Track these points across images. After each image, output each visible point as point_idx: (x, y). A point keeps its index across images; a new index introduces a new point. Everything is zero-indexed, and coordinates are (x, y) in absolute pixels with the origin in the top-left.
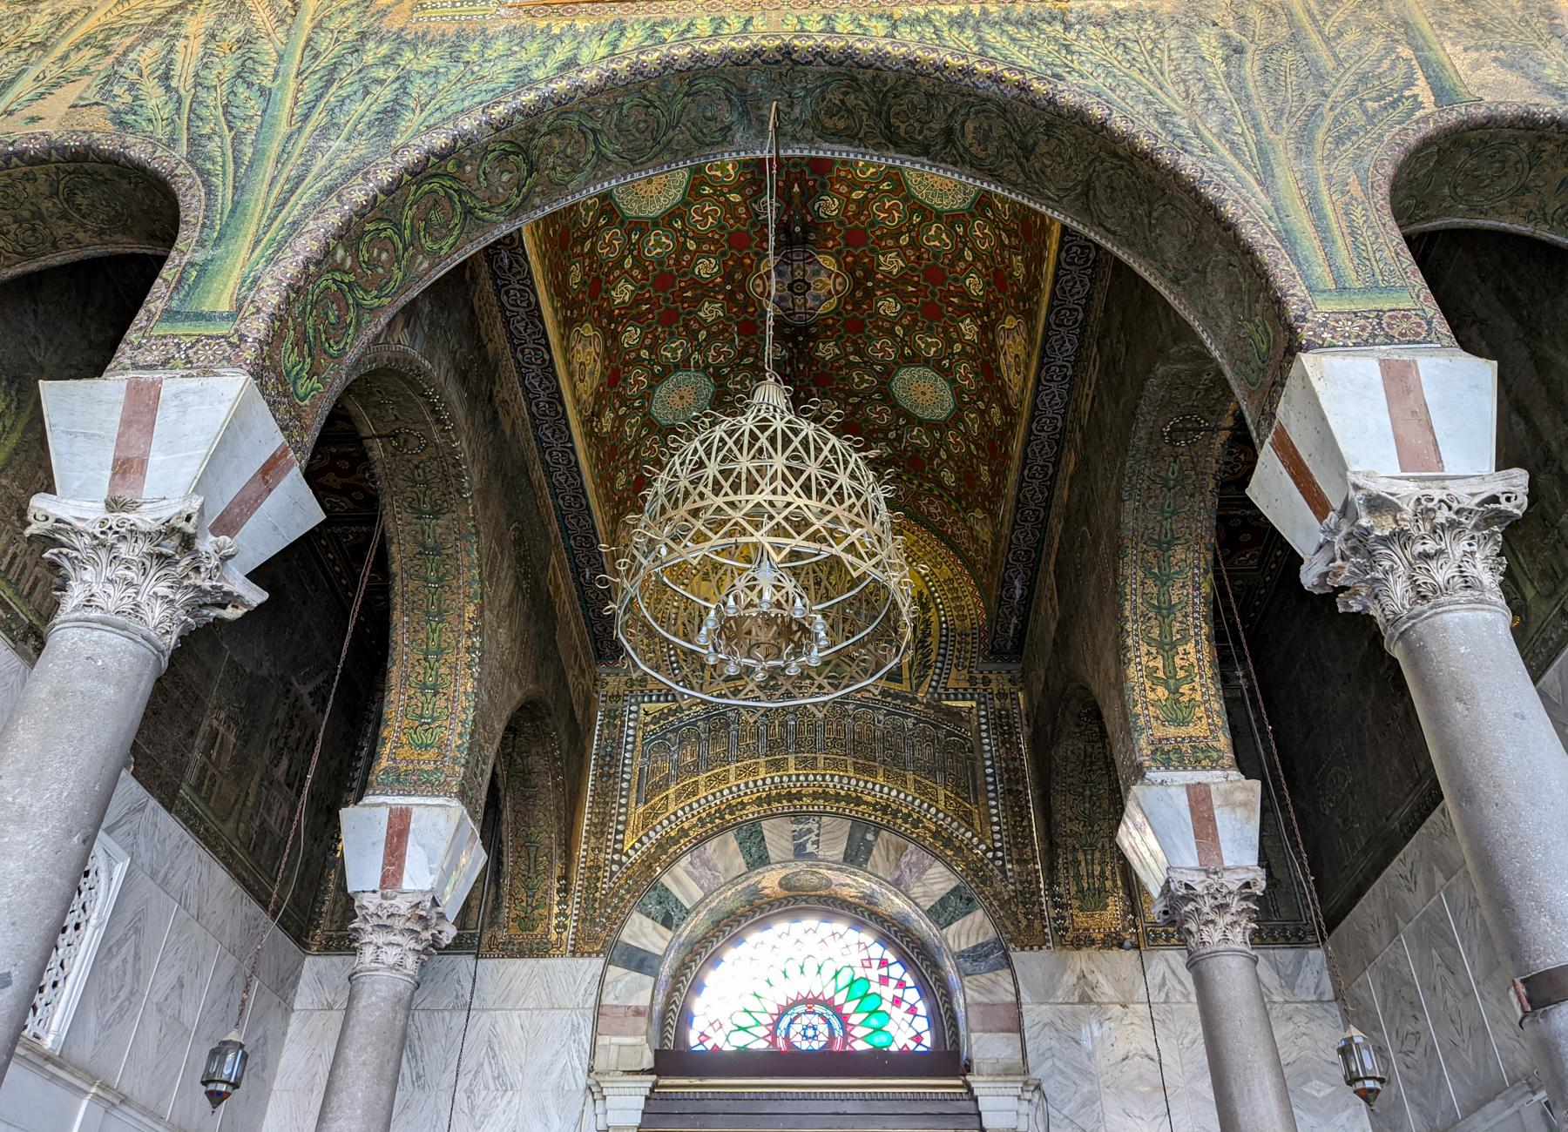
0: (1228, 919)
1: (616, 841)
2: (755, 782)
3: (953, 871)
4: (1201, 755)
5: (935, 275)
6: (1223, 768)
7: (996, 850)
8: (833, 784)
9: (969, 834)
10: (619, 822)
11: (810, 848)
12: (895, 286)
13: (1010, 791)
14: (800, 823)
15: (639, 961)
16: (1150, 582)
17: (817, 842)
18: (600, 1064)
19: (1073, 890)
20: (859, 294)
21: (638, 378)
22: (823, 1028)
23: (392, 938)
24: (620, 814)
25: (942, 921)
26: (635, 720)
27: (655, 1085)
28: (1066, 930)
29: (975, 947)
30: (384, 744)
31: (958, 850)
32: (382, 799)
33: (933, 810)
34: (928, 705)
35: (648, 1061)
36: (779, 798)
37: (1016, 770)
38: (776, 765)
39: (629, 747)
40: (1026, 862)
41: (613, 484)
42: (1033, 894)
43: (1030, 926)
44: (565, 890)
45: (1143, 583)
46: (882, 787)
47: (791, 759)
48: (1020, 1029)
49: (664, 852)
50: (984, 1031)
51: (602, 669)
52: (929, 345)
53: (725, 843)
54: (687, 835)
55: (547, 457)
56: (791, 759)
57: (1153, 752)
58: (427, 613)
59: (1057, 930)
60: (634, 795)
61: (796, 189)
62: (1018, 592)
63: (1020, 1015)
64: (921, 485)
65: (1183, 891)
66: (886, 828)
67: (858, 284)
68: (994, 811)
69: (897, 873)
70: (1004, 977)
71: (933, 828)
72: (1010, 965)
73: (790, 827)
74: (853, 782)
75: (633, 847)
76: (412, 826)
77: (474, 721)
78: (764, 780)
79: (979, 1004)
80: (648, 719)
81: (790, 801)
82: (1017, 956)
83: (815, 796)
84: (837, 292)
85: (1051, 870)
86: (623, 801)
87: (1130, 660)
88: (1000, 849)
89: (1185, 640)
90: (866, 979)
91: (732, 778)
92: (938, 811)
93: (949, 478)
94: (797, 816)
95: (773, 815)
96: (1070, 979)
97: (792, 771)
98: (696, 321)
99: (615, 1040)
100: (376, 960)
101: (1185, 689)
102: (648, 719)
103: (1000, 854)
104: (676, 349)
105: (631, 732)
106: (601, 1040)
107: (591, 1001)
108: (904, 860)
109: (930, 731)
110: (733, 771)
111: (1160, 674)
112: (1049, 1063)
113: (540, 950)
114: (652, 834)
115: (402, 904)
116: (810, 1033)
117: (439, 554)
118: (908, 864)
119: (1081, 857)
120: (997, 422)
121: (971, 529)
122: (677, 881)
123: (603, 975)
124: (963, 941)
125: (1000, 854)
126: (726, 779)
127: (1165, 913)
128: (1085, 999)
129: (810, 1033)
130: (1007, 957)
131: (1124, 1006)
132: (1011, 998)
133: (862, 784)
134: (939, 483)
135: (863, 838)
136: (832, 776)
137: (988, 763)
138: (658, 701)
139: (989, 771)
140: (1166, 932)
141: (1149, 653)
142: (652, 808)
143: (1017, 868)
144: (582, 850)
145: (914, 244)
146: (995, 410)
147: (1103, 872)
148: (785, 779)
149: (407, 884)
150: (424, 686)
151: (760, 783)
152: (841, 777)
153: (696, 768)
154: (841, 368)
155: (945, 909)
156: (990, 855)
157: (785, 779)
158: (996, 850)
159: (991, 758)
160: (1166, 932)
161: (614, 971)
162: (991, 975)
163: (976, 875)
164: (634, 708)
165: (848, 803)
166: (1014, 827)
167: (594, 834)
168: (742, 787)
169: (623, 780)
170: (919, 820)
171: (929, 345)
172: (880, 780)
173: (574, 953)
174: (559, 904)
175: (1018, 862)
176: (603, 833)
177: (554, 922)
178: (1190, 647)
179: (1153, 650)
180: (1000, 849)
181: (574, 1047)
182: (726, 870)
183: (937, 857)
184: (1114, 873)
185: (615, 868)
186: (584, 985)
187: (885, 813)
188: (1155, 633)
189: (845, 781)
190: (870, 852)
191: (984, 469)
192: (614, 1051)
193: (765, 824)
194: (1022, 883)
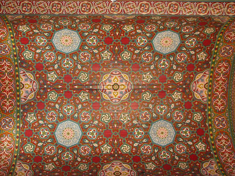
5: (108, 41)
12: (116, 54)
64: (219, 41)
93: (209, 31)
134: (214, 34)
145: (97, 47)
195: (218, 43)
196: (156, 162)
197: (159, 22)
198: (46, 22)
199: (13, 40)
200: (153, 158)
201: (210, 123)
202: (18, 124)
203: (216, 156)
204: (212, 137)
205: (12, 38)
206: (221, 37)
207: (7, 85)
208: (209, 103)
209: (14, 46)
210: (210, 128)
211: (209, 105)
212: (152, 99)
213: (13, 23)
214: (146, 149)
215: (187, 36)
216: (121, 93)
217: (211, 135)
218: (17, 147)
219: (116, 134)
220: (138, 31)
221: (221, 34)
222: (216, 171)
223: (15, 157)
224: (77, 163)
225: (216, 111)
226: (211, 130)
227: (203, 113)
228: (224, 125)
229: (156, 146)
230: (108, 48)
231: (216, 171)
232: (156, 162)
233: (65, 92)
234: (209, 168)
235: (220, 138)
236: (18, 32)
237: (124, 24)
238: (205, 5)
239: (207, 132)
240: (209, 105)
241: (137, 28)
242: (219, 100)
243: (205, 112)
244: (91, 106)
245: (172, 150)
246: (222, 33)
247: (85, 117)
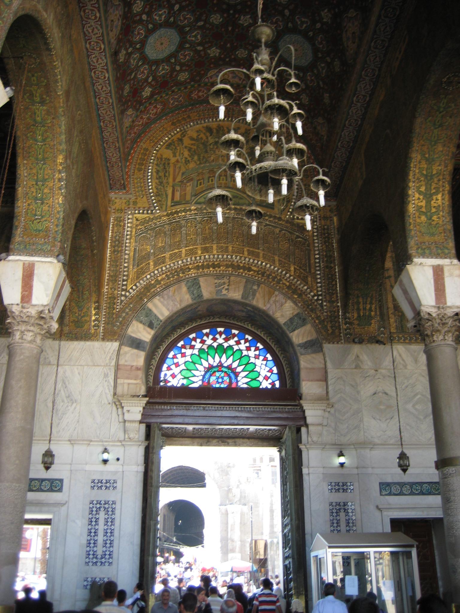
0: (446, 329)
1: (123, 285)
2: (196, 257)
3: (296, 305)
4: (440, 251)
6: (450, 258)
7: (318, 296)
8: (236, 259)
9: (306, 287)
10: (124, 276)
11: (224, 292)
13: (327, 267)
14: (219, 279)
15: (137, 344)
16: (423, 162)
18: (119, 390)
19: (356, 315)
21: (140, 31)
22: (226, 379)
23: (29, 328)
24: (124, 271)
26: (131, 223)
27: (148, 403)
28: (351, 334)
29: (306, 342)
30: (17, 229)
31: (300, 295)
32: (18, 258)
33: (288, 275)
34: (287, 222)
35: (143, 391)
36: (208, 267)
37: (331, 257)
38: (205, 250)
39: (128, 237)
40: (333, 302)
41: (123, 92)
42: (336, 317)
43: (333, 332)
44: (98, 308)
45: (420, 162)
46: (262, 263)
47: (215, 246)
48: (326, 380)
49: (148, 292)
50: (308, 380)
51: (112, 195)
52: (302, 23)
53: (180, 288)
54: (160, 283)
55: (93, 74)
56: (215, 246)
57: (417, 249)
58: (37, 159)
59: (346, 334)
60: (132, 262)
65: (427, 316)
66: (263, 283)
68: (319, 277)
69: (268, 306)
70: (318, 357)
71: (288, 284)
73: (213, 281)
74: (247, 259)
75: (132, 288)
76: (36, 272)
77: (63, 218)
78: (200, 257)
79: (307, 368)
80: (138, 223)
81: (214, 268)
82: (327, 347)
83: (227, 266)
85: (345, 306)
86: (126, 265)
87: (409, 202)
88: (321, 295)
89: (437, 193)
90: (248, 356)
91: (183, 255)
92: (290, 276)
94: (218, 276)
95: (206, 275)
96: (351, 357)
97: (215, 252)
99: (127, 381)
100: (22, 338)
101: (435, 218)
102: (138, 223)
103: (320, 298)
104: (161, 15)
105: (129, 229)
106: (119, 381)
107: (113, 363)
108: (273, 299)
109: (288, 235)
110: (183, 250)
111: (424, 210)
112: (339, 395)
113: (86, 337)
114: (141, 282)
115: (33, 312)
116: (220, 380)
117: (44, 126)
119: (361, 300)
120: (337, 69)
121: (315, 128)
122: (156, 306)
123: (119, 350)
124: (300, 339)
125: (320, 298)
126: (180, 256)
127: (415, 326)
128: (357, 367)
129: (220, 380)
131: (376, 371)
133: (251, 261)
135: (251, 288)
136: (236, 256)
137: (317, 252)
138: (143, 213)
139: (317, 256)
140: (398, 337)
141: (419, 199)
142: (142, 268)
144: (105, 289)
146: (337, 63)
147: (371, 308)
148: (212, 257)
149: (34, 301)
150: (36, 199)
151: (198, 258)
152: (241, 257)
153: (163, 250)
155: (292, 323)
156: (316, 298)
157: (212, 257)
158: (318, 296)
159: (318, 250)
160: (398, 337)
161: (125, 349)
163: (308, 307)
164: (130, 217)
165: (244, 270)
166: (328, 284)
167: (112, 281)
168: (189, 259)
169: (126, 254)
170: (280, 280)
171: (302, 23)
172: (261, 259)
173: (103, 339)
174: (95, 315)
175: (329, 302)
176: (116, 281)
177: (93, 324)
178: (439, 197)
179: (421, 197)
180: (321, 295)
181: (106, 384)
182: (181, 301)
183: (289, 298)
184: (376, 308)
185: (123, 298)
186: (110, 355)
187: (263, 276)
188: (423, 189)
189: (243, 259)
191: (326, 95)
192: (126, 387)
193: (202, 280)
194: (330, 312)
208: (202, 85)
210: (170, 93)
211: (199, 85)
217: (161, 97)
225: (191, 92)
226: (167, 94)
227: (188, 81)
235: (158, 107)
239: (164, 92)
240: (199, 85)
242: (206, 93)
243: (189, 83)
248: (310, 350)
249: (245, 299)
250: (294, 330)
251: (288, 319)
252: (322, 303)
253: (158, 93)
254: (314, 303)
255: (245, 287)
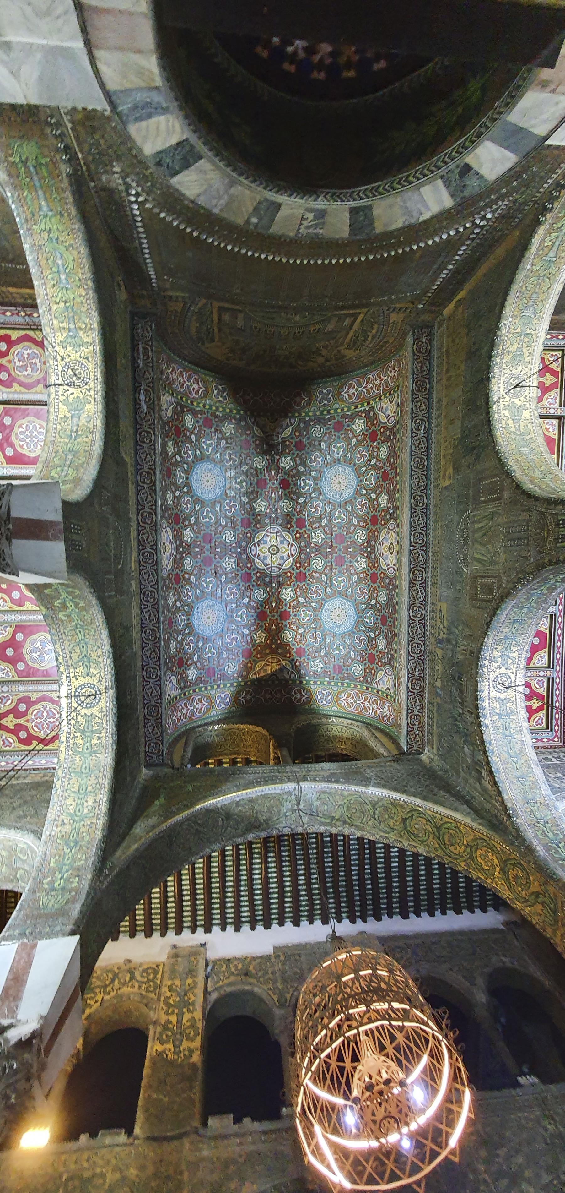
5: (207, 562)
7: (136, 202)
17: (303, 219)
20: (244, 544)
25: (187, 148)
29: (149, 116)
61: (274, 605)
62: (142, 397)
63: (84, 30)
64: (204, 406)
67: (245, 550)
69: (233, 190)
72: (108, 95)
84: (254, 545)
93: (189, 421)
98: (326, 532)
118: (220, 197)
124: (163, 127)
130: (113, 106)
132: (99, 54)
134: (195, 413)
135: (260, 219)
143: (113, 185)
154: (252, 493)
155: (184, 158)
156: (141, 199)
162: (128, 86)
190: (256, 209)
195: (207, 407)
196: (378, 492)
197: (177, 493)
198: (182, 645)
199: (209, 688)
200: (373, 496)
201: (325, 413)
202: (326, 683)
203: (371, 402)
204: (346, 409)
205: (206, 688)
206: (198, 403)
207: (273, 696)
209: (219, 686)
210: (332, 412)
212: (291, 498)
213: (185, 687)
214: (361, 507)
215: (198, 452)
216: (282, 542)
217: (342, 410)
218: (356, 686)
219: (340, 550)
220: (192, 522)
221: (195, 404)
222: (391, 402)
223: (367, 689)
224: (378, 605)
226: (336, 409)
228: (329, 392)
229: (357, 493)
230: (218, 562)
231: (391, 402)
232: (378, 492)
233: (281, 620)
234: (387, 413)
236: (198, 680)
237: (182, 542)
238: (140, 434)
240: (300, 415)
241: (187, 523)
244: (301, 585)
245: (364, 469)
246: (192, 403)
247: (316, 592)
248: (140, 97)
249: (273, 203)
250: (178, 144)
251: (193, 167)
252: (127, 190)
253: (345, 416)
254: (143, 190)
255: (272, 221)
